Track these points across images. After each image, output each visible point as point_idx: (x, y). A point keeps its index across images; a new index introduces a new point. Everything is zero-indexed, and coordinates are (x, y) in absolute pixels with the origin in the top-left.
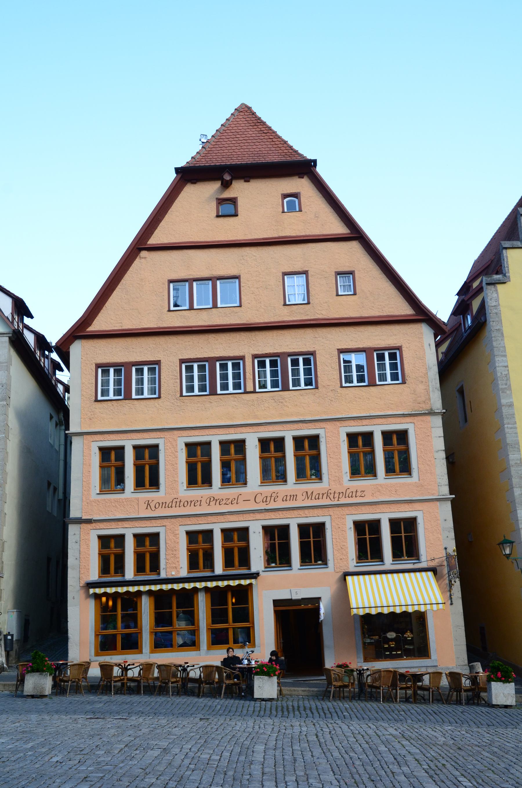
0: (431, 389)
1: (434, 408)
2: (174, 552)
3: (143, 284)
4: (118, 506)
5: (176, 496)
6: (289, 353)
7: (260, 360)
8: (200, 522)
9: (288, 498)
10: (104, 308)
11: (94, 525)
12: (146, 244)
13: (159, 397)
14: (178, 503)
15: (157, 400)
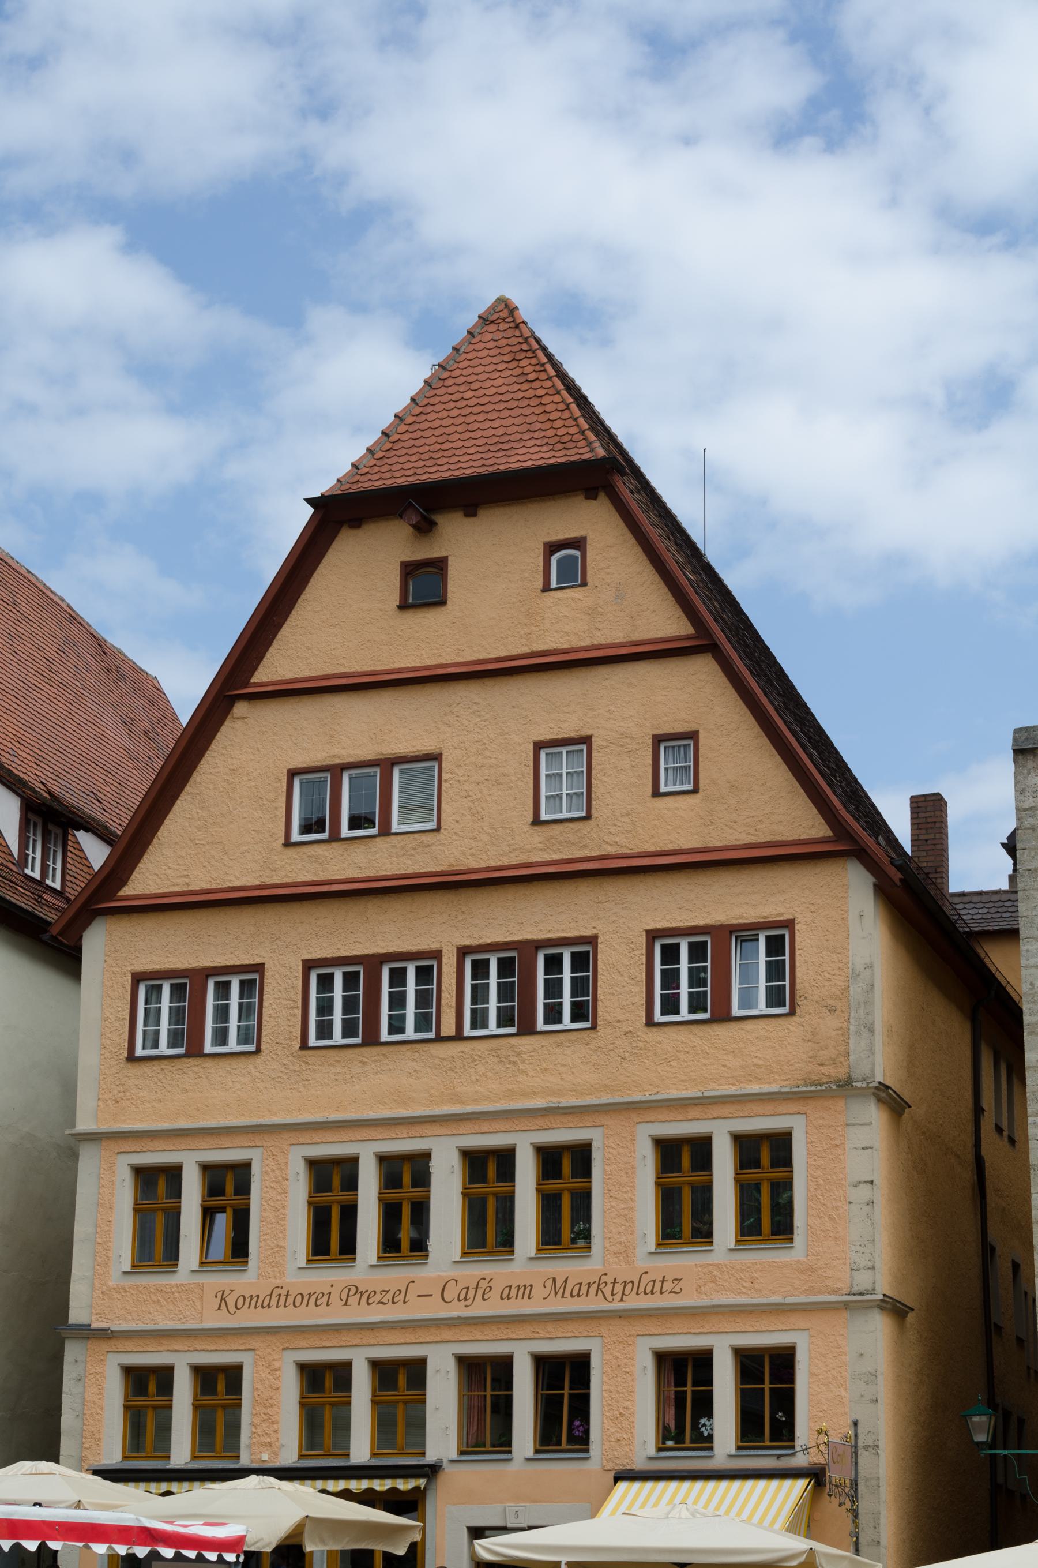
0: (852, 1028)
1: (855, 1076)
2: (269, 1411)
3: (237, 780)
4: (162, 1300)
6: (538, 941)
7: (475, 959)
10: (155, 841)
11: (112, 1342)
12: (247, 684)
13: (258, 1051)
14: (283, 1298)
15: (252, 1058)
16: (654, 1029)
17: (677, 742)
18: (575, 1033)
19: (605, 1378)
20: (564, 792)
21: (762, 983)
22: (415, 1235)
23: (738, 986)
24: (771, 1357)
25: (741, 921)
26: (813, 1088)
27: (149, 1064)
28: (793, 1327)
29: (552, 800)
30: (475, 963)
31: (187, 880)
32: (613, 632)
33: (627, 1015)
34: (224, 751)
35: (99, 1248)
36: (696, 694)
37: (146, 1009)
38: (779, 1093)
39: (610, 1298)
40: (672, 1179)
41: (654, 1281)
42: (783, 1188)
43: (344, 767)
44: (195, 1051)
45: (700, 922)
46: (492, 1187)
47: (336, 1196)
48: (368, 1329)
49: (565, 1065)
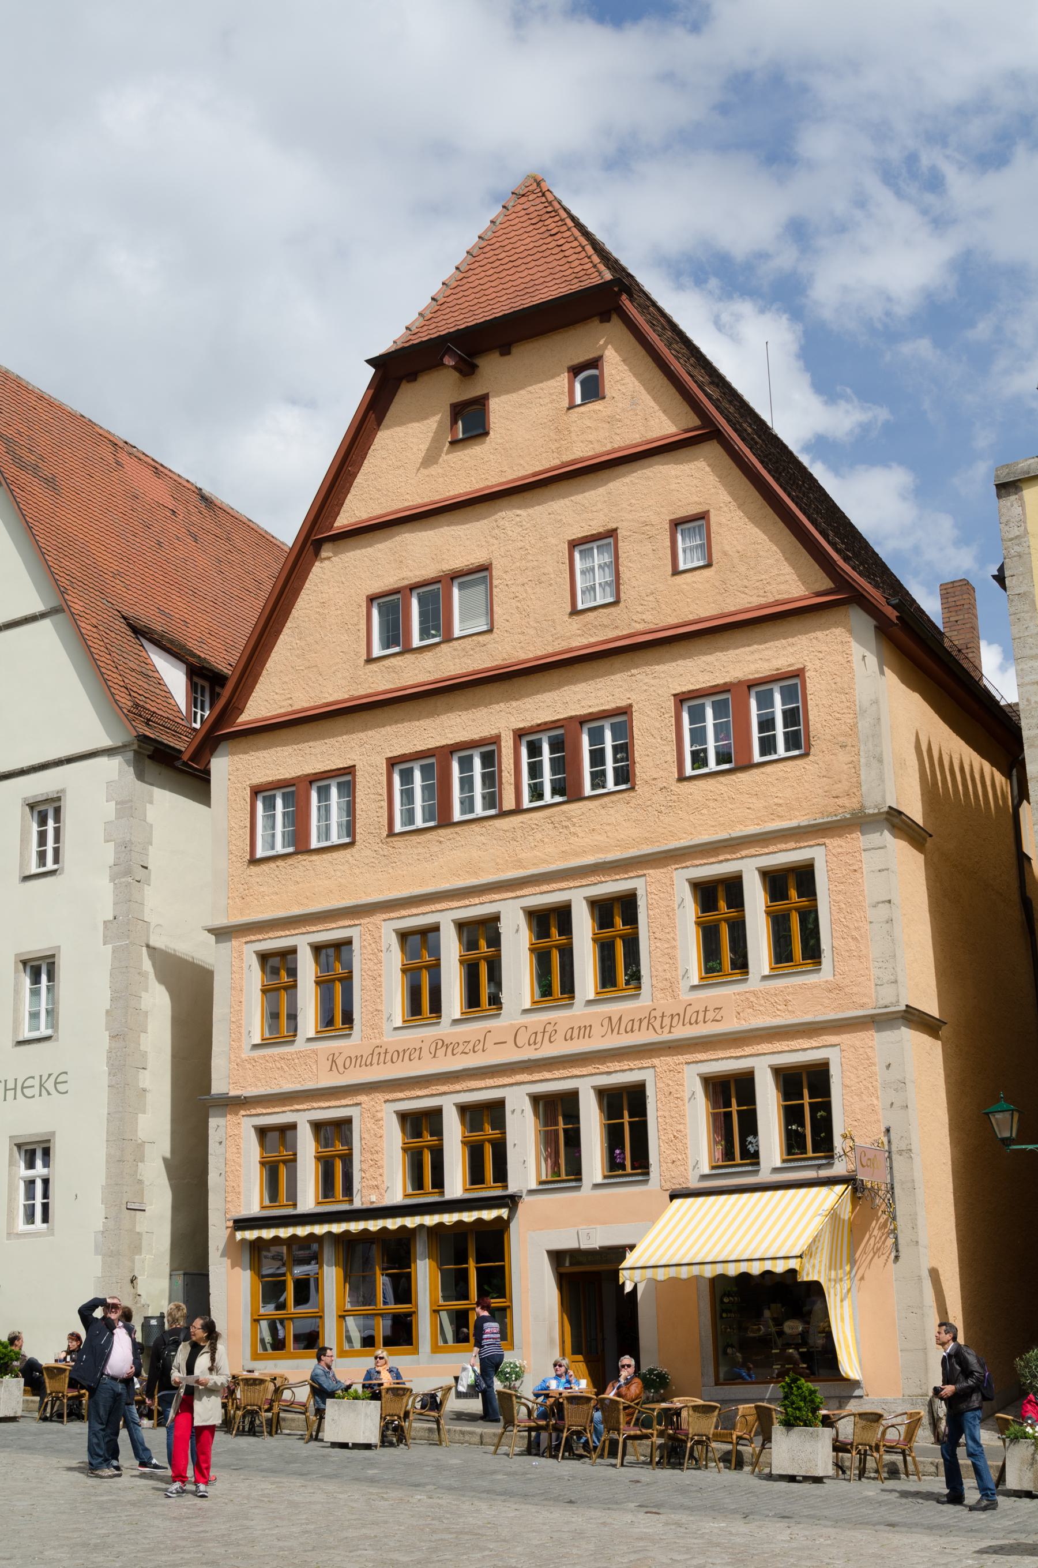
0: (862, 760)
1: (867, 804)
2: (375, 1157)
3: (326, 611)
4: (285, 1067)
5: (378, 1042)
7: (528, 738)
9: (576, 1032)
10: (264, 672)
17: (692, 523)
20: (597, 582)
22: (493, 990)
25: (756, 676)
28: (826, 1043)
31: (290, 702)
35: (234, 1026)
39: (659, 1031)
41: (698, 1012)
43: (412, 588)
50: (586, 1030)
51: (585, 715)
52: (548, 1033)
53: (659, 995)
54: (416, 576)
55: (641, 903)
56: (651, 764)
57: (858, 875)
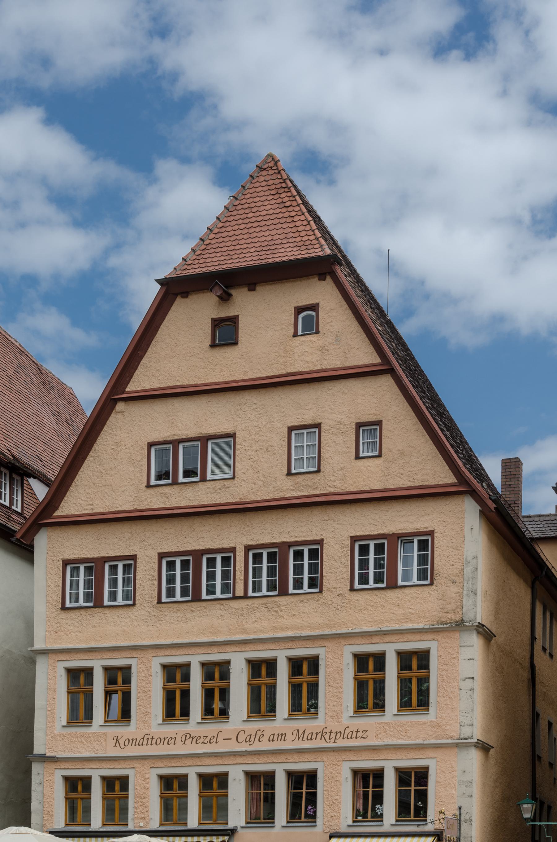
0: (465, 592)
1: (465, 619)
2: (143, 800)
3: (119, 449)
4: (84, 741)
5: (147, 732)
6: (290, 542)
7: (254, 552)
8: (173, 765)
9: (276, 737)
10: (73, 484)
11: (58, 764)
13: (134, 604)
14: (150, 741)
15: (131, 609)
16: (354, 593)
18: (310, 595)
19: (325, 784)
20: (305, 456)
21: (415, 567)
23: (402, 568)
24: (415, 772)
25: (404, 531)
26: (442, 626)
27: (74, 611)
28: (428, 757)
29: (298, 461)
30: (255, 555)
31: (92, 507)
32: (334, 362)
33: (339, 584)
34: (111, 432)
35: (49, 713)
36: (380, 399)
37: (71, 580)
38: (423, 628)
39: (328, 741)
40: (363, 676)
42: (424, 681)
44: (99, 604)
45: (381, 532)
46: (264, 680)
47: (178, 685)
48: (197, 757)
49: (304, 613)
50: (282, 736)
51: (293, 542)
52: (258, 736)
53: (330, 720)
54: (183, 435)
55: (322, 663)
56: (334, 579)
57: (456, 661)
